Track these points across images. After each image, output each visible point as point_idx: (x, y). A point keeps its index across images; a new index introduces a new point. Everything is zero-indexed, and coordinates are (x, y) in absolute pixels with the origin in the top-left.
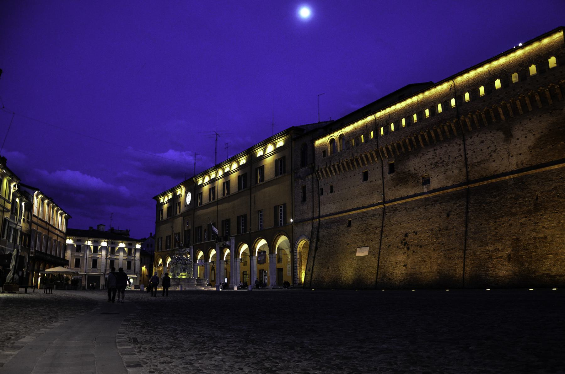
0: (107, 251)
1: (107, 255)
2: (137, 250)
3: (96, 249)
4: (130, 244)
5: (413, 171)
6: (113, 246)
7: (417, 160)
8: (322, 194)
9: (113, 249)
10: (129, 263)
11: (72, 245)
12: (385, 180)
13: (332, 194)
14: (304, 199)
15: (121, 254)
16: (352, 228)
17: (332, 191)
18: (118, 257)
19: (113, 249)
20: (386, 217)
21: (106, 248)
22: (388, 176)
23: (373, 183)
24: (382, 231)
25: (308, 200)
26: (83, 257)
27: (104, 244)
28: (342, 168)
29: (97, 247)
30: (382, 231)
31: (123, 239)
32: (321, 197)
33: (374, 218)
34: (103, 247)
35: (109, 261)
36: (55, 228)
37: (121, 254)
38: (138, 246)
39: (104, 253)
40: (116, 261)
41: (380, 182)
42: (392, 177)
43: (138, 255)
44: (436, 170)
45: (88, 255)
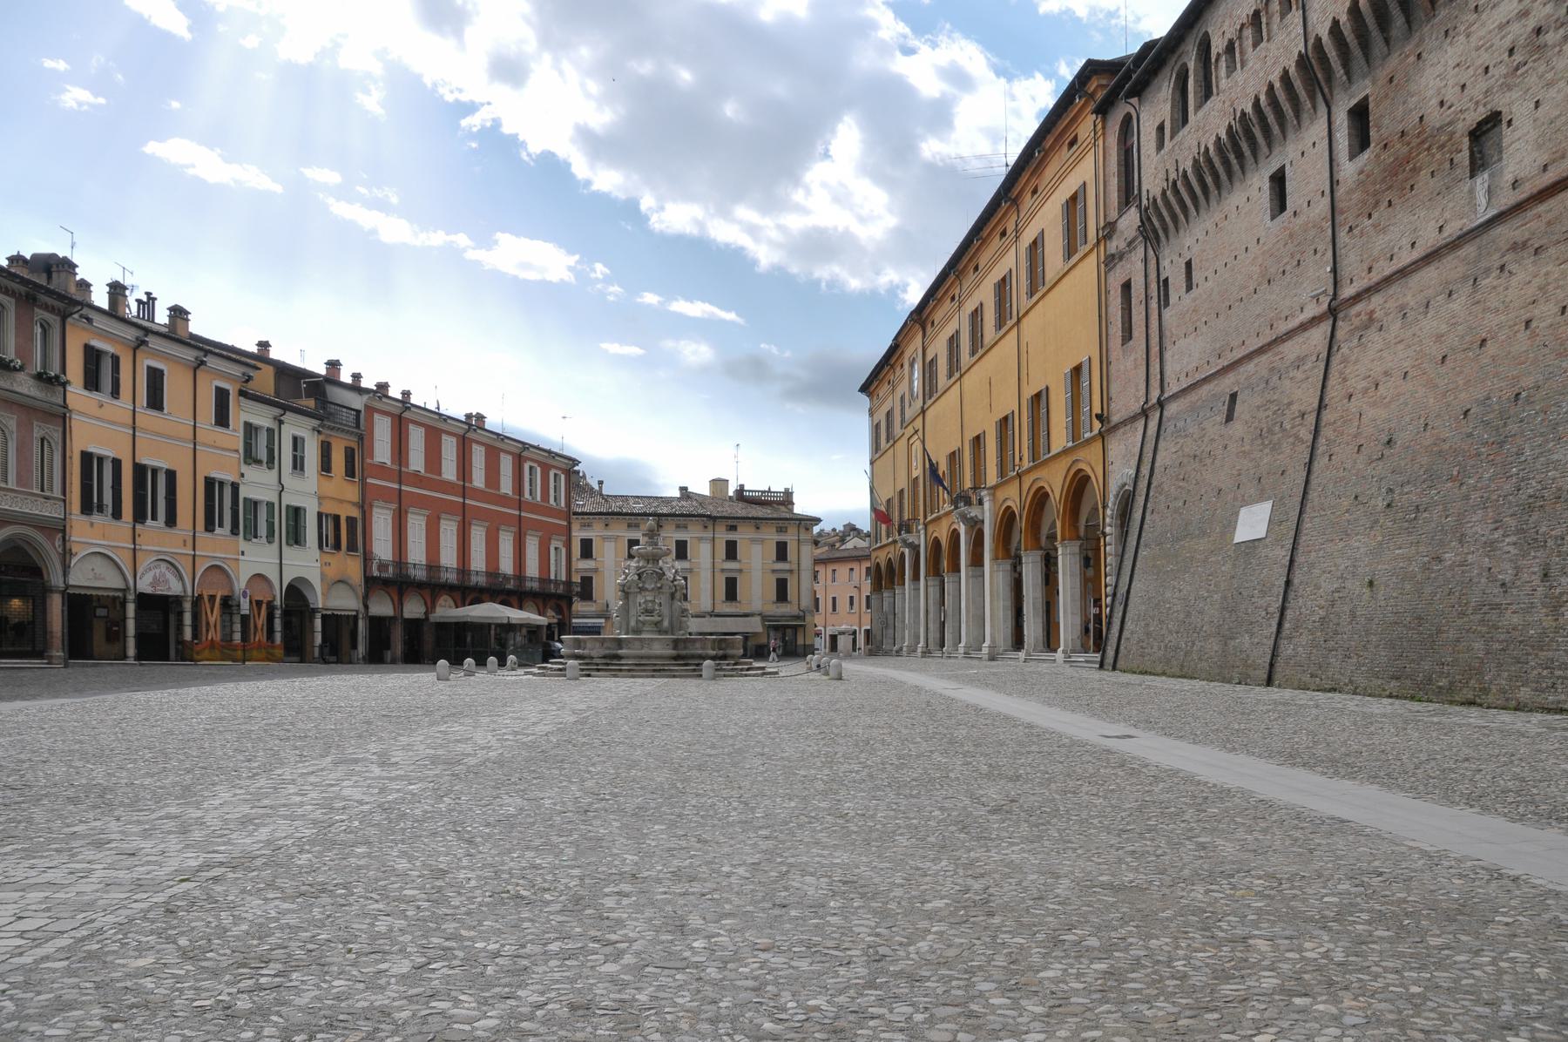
5: (1435, 117)
7: (1452, 52)
8: (1167, 304)
12: (1341, 191)
13: (1195, 292)
14: (1127, 334)
16: (1237, 428)
17: (1189, 288)
20: (1335, 360)
22: (1349, 169)
23: (1300, 221)
24: (1316, 432)
25: (1135, 333)
28: (1209, 180)
30: (1316, 432)
32: (1167, 313)
33: (1299, 375)
41: (1327, 199)
42: (1361, 172)
44: (1532, 79)
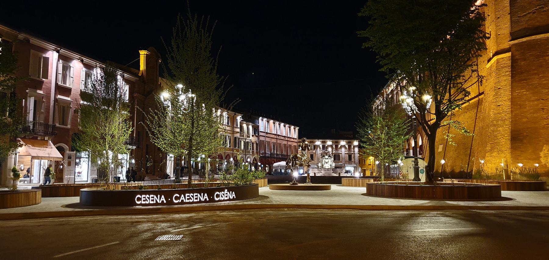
0: (332, 148)
2: (354, 147)
3: (324, 147)
4: (349, 142)
6: (336, 144)
9: (336, 146)
10: (350, 157)
15: (343, 149)
19: (336, 146)
21: (331, 146)
31: (343, 139)
34: (328, 146)
36: (285, 137)
37: (343, 149)
38: (356, 143)
43: (356, 150)
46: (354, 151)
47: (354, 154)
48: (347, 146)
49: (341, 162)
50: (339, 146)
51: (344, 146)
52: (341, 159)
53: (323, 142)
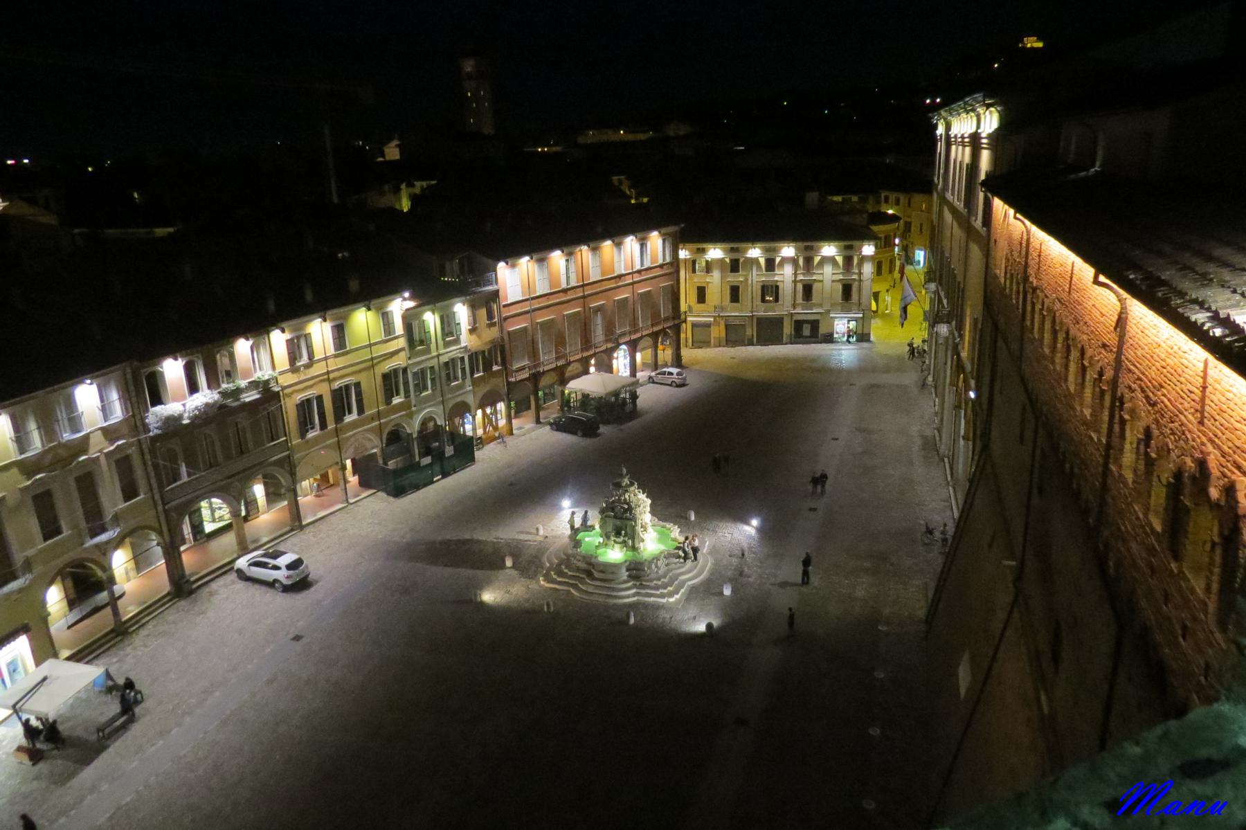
1: (795, 275)
2: (863, 259)
3: (770, 265)
6: (808, 254)
9: (808, 261)
10: (847, 290)
11: (722, 260)
18: (820, 278)
21: (794, 261)
26: (747, 280)
27: (788, 251)
29: (773, 260)
34: (784, 260)
35: (800, 287)
37: (828, 269)
39: (788, 270)
40: (816, 287)
43: (868, 269)
45: (756, 278)
46: (860, 274)
47: (860, 280)
48: (839, 259)
49: (821, 305)
50: (817, 259)
51: (832, 260)
52: (816, 298)
53: (767, 250)
